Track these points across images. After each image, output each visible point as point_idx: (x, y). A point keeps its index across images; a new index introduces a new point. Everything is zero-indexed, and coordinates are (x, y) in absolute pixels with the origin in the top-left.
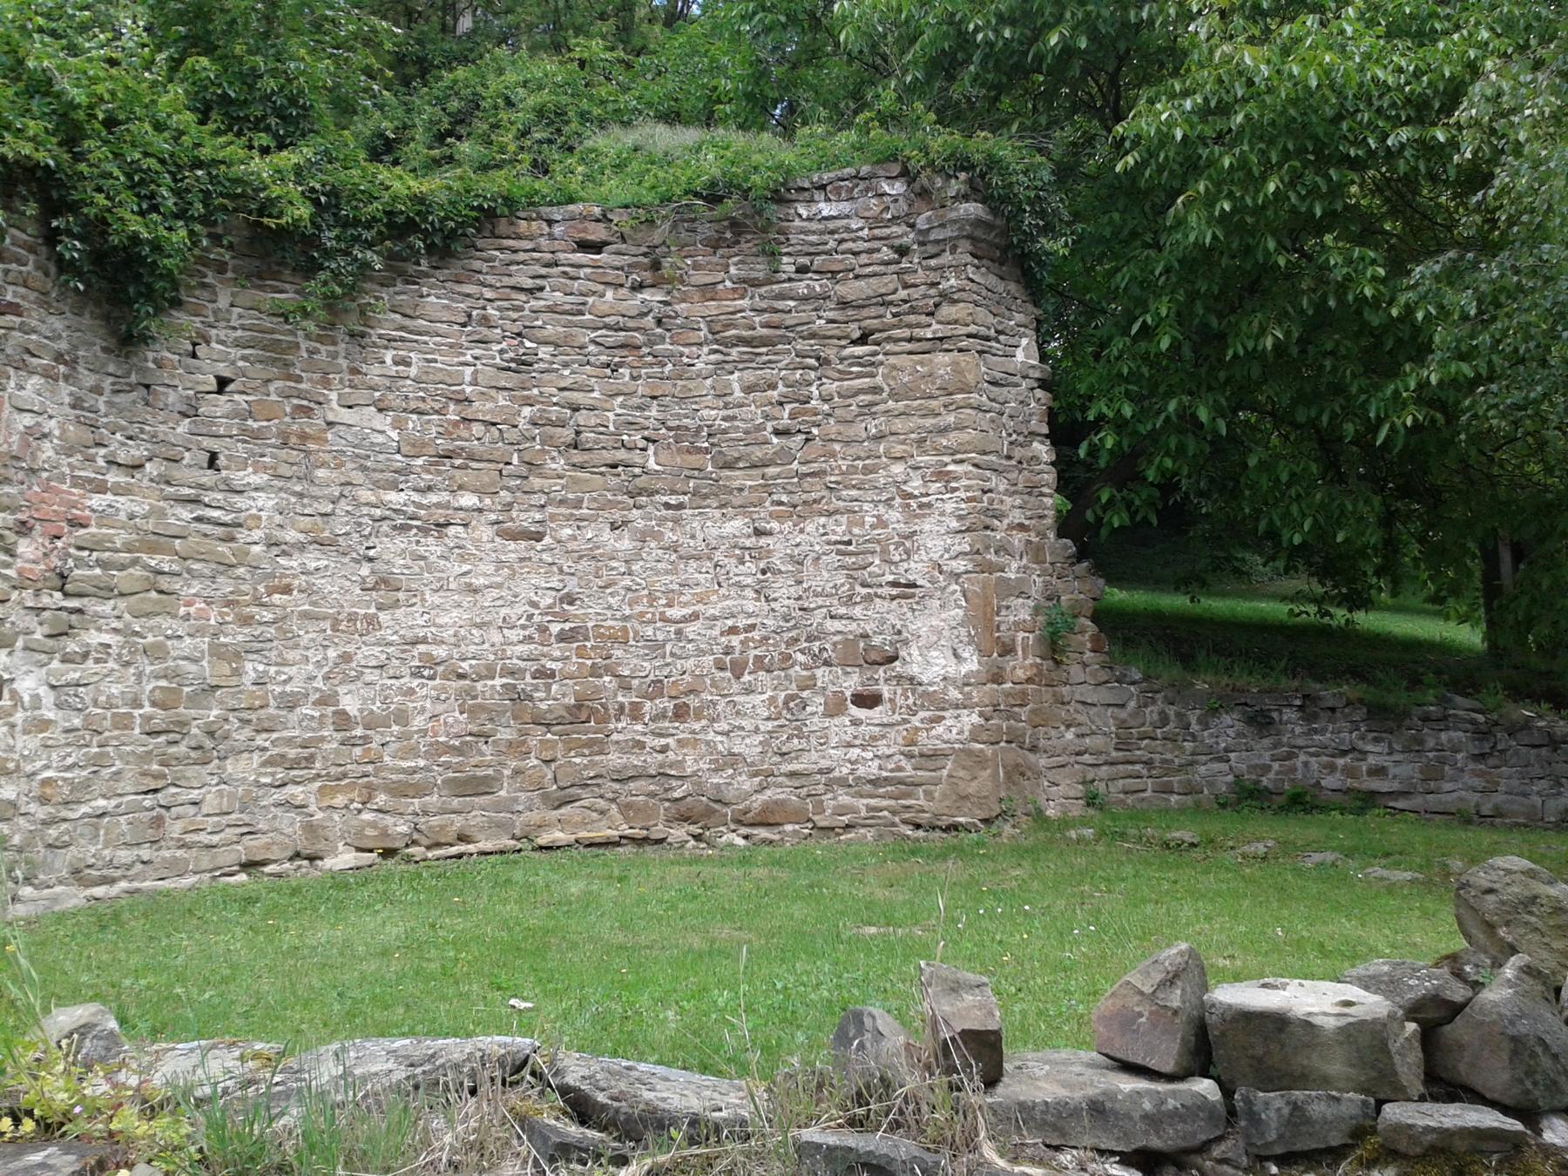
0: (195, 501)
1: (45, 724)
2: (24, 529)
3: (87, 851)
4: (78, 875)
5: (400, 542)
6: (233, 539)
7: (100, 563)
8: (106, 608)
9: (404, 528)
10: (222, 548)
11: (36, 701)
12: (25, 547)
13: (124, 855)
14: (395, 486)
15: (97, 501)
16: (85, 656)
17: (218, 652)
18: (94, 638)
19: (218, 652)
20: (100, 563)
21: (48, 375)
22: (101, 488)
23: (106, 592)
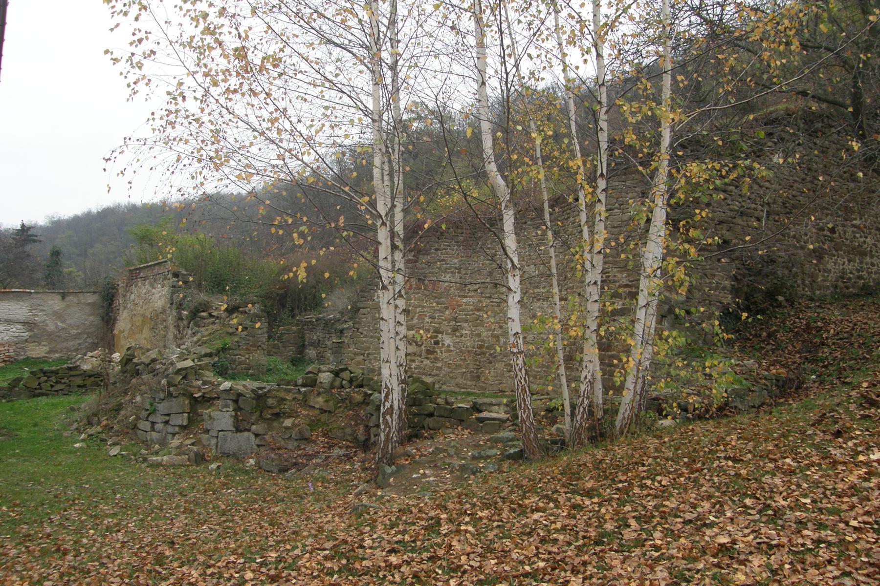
0: (490, 297)
1: (451, 351)
2: (447, 308)
3: (460, 380)
4: (457, 385)
5: (539, 304)
6: (499, 306)
7: (466, 315)
8: (466, 325)
9: (539, 300)
10: (496, 309)
11: (449, 346)
12: (447, 312)
13: (469, 383)
14: (537, 287)
15: (465, 300)
16: (462, 336)
17: (493, 336)
18: (464, 332)
19: (493, 336)
20: (466, 315)
21: (452, 272)
22: (466, 297)
23: (466, 321)
